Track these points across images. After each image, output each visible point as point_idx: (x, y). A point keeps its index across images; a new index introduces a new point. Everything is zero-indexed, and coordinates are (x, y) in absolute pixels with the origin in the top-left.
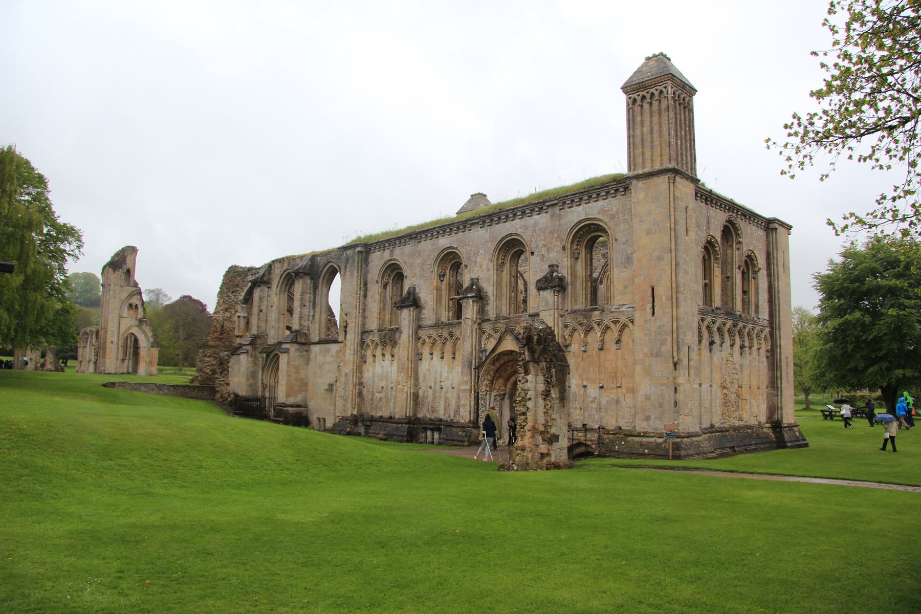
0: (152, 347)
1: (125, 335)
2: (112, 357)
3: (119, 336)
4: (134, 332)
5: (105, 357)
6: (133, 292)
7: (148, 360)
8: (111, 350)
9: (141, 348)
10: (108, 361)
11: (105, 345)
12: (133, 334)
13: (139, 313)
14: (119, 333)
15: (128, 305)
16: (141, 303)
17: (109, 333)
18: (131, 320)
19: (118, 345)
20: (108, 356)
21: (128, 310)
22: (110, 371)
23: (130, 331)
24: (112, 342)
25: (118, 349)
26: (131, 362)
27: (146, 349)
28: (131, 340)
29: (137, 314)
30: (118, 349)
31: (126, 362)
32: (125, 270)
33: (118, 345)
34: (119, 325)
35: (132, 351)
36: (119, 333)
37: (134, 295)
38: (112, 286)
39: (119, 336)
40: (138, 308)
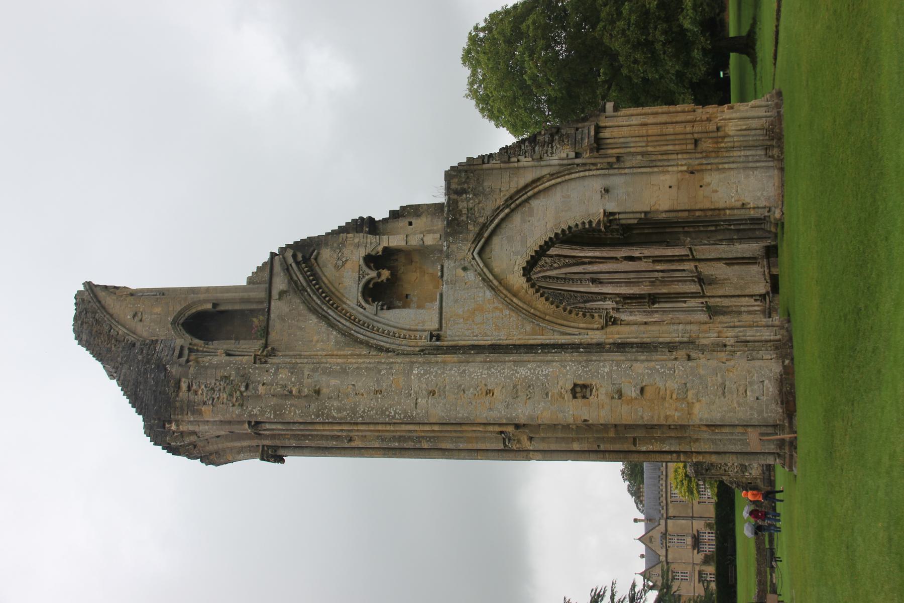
0: (599, 144)
1: (541, 304)
2: (672, 385)
3: (547, 348)
4: (521, 262)
5: (683, 427)
6: (295, 287)
7: (682, 163)
8: (631, 392)
9: (612, 207)
10: (701, 413)
11: (605, 427)
12: (527, 271)
13: (414, 241)
14: (530, 348)
15: (371, 309)
16: (358, 238)
17: (523, 412)
18: (453, 283)
19: (599, 347)
20: (672, 413)
21: (405, 305)
22: (771, 388)
23: (517, 280)
24: (580, 391)
25: (621, 347)
26: (704, 250)
27: (608, 182)
28: (592, 261)
29: (423, 251)
30: (621, 347)
31: (707, 270)
32: (183, 340)
33: (599, 347)
34: (478, 349)
35: (648, 252)
36: (530, 348)
37: (314, 278)
38: (254, 410)
39: (547, 348)
40: (389, 252)
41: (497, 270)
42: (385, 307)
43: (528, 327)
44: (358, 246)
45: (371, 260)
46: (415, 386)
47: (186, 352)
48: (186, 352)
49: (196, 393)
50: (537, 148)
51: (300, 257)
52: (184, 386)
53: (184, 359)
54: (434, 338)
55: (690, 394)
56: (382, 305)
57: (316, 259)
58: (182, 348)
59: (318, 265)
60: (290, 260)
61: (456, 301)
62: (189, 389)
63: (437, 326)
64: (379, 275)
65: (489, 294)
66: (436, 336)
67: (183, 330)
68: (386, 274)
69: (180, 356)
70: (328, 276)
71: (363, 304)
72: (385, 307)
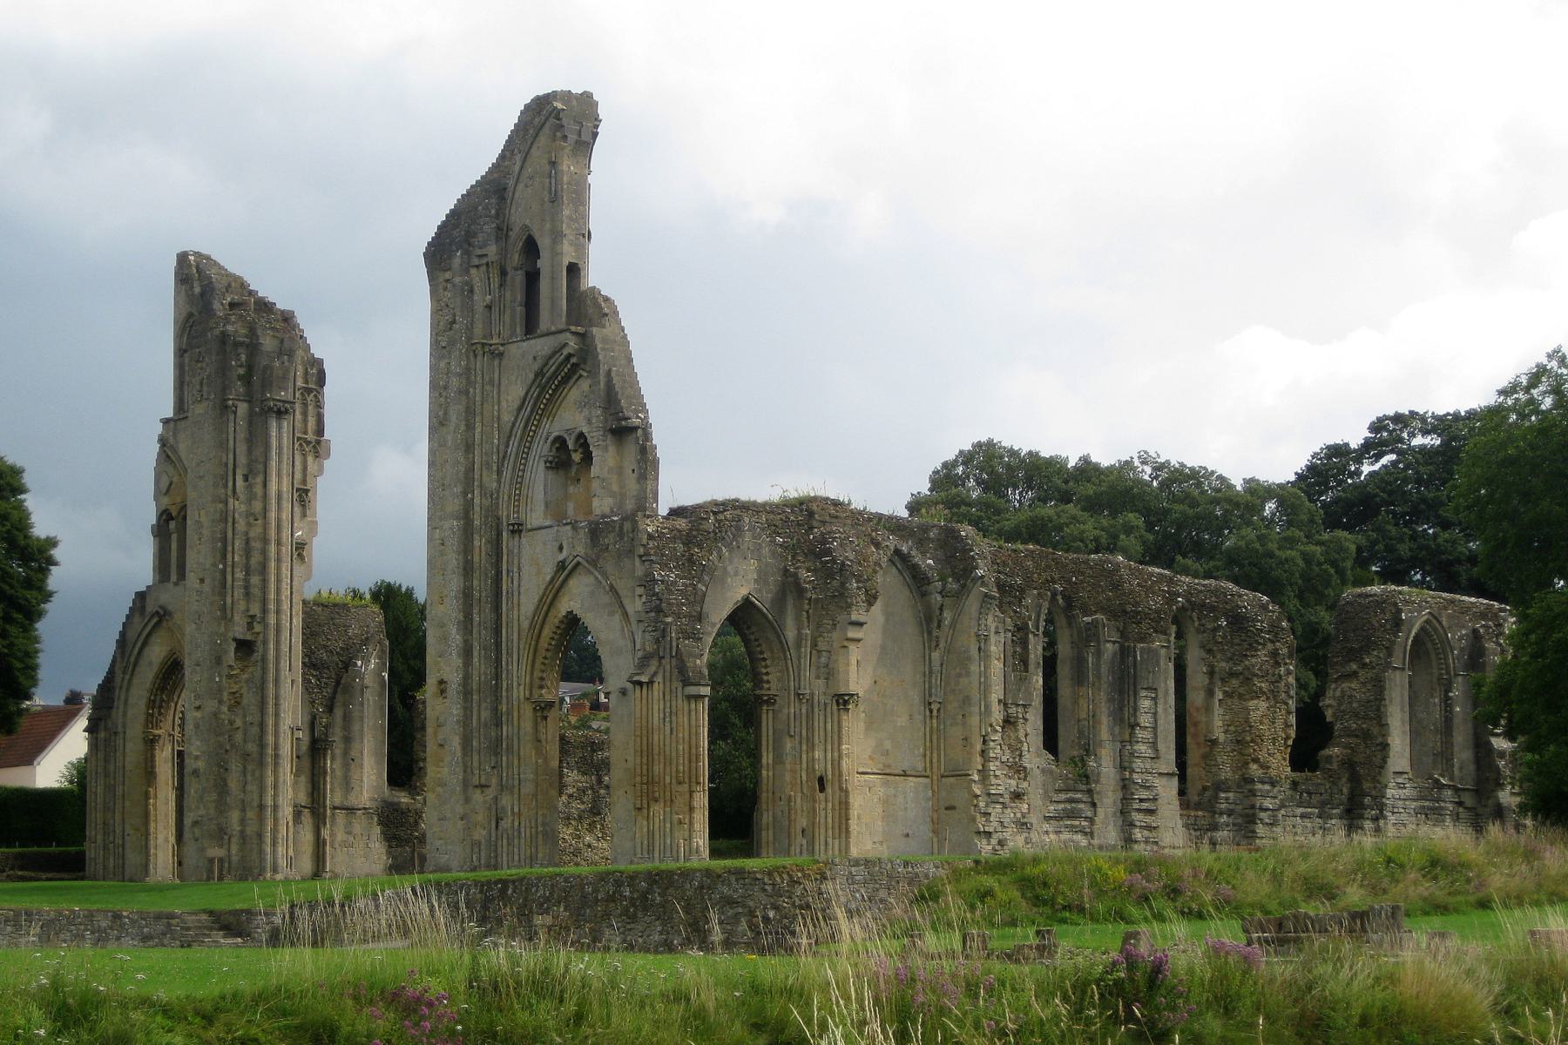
41: (572, 582)
42: (548, 465)
43: (525, 624)
44: (589, 421)
45: (582, 441)
46: (447, 525)
47: (484, 261)
48: (484, 261)
49: (445, 289)
50: (653, 614)
51: (574, 360)
52: (448, 275)
53: (476, 261)
54: (511, 528)
55: (439, 789)
56: (551, 462)
57: (581, 376)
58: (486, 255)
59: (577, 380)
60: (565, 352)
61: (545, 544)
62: (447, 281)
63: (529, 526)
64: (576, 451)
65: (548, 578)
66: (517, 530)
67: (524, 237)
68: (577, 457)
69: (480, 256)
70: (571, 393)
71: (551, 439)
72: (548, 465)
